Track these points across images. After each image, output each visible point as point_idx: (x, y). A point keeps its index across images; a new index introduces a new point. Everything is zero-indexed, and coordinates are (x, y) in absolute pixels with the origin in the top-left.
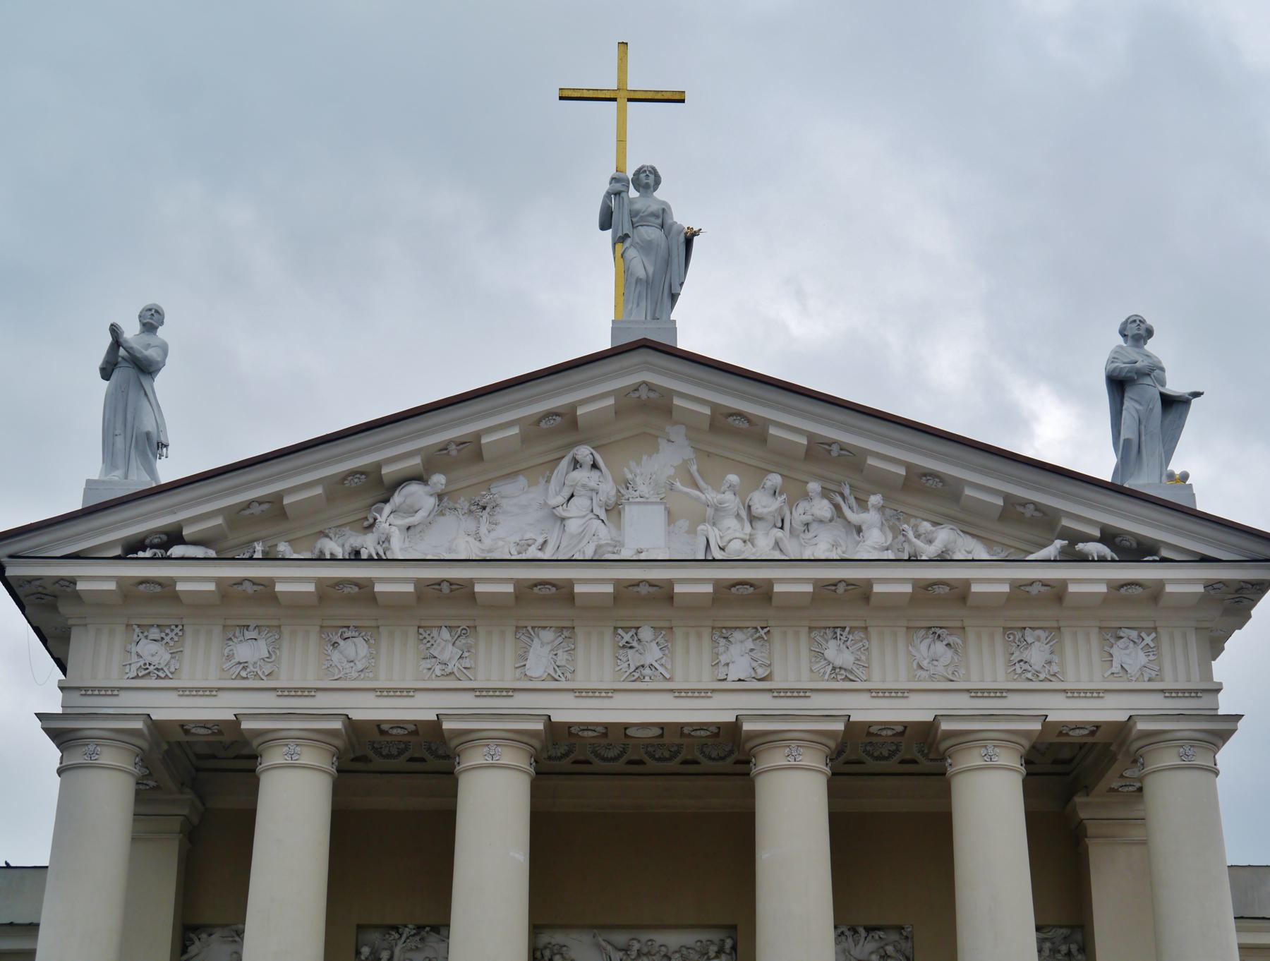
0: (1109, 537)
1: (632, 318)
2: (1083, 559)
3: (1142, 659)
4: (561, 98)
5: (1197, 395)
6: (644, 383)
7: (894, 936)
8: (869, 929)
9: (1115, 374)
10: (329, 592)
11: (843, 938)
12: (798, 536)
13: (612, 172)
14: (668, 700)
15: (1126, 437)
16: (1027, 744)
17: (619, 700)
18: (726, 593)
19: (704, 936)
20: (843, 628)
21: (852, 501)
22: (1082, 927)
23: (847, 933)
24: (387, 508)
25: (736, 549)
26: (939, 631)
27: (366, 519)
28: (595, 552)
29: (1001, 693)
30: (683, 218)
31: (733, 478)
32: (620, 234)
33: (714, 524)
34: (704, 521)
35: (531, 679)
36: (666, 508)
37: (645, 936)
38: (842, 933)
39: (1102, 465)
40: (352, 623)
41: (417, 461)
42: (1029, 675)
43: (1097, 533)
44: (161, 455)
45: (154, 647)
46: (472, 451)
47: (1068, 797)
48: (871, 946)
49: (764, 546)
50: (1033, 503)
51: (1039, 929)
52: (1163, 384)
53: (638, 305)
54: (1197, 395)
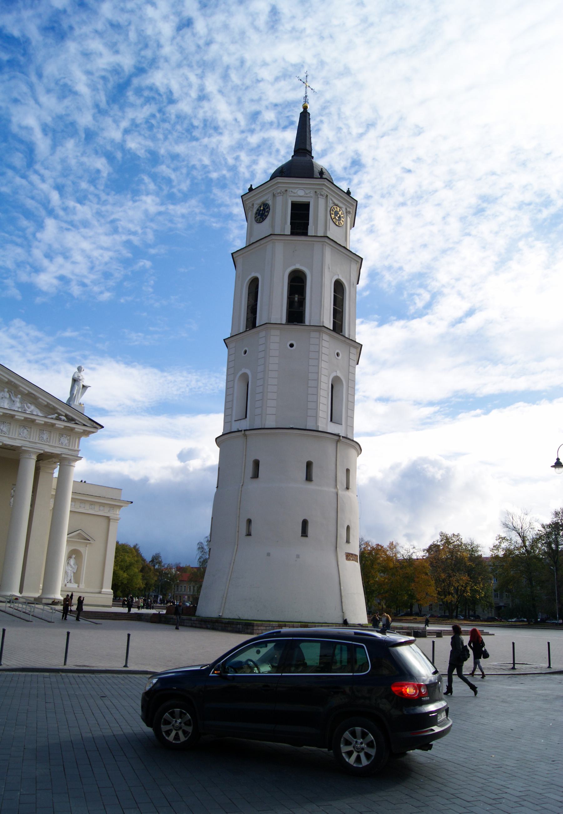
0: (66, 416)
3: (66, 441)
5: (90, 387)
20: (6, 422)
21: (13, 394)
29: (35, 443)
42: (43, 440)
43: (64, 415)
52: (83, 382)
54: (90, 387)
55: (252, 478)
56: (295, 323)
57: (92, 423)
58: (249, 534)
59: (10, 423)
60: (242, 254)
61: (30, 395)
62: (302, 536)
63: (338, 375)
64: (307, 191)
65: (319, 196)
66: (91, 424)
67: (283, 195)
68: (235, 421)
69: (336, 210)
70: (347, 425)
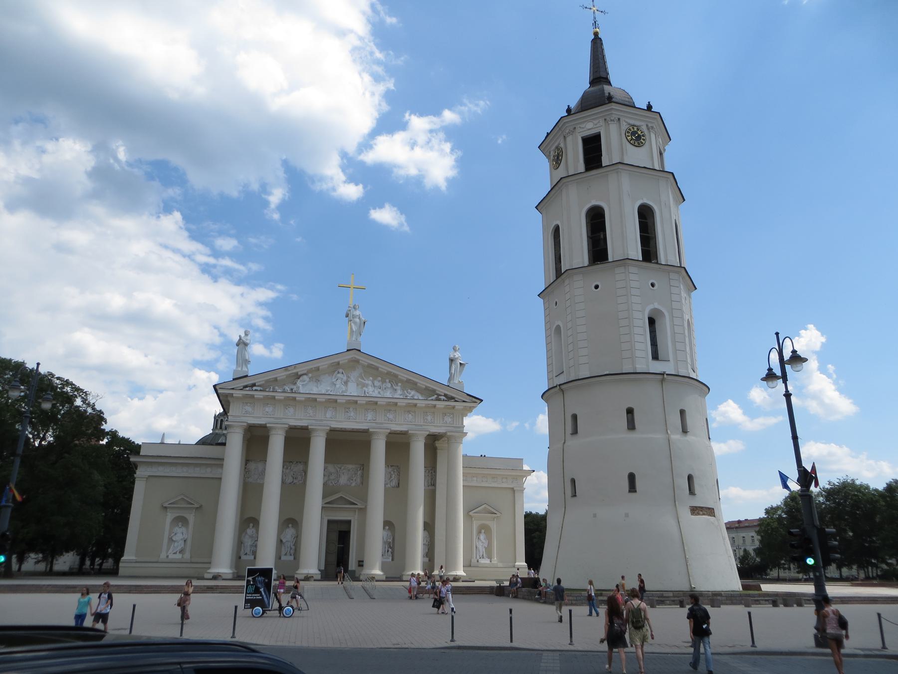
0: (445, 395)
2: (440, 400)
3: (450, 420)
8: (391, 466)
10: (287, 398)
18: (368, 403)
29: (421, 425)
31: (371, 378)
33: (367, 387)
34: (364, 386)
35: (326, 417)
46: (318, 369)
47: (435, 441)
49: (376, 394)
55: (572, 434)
56: (596, 263)
57: (471, 398)
58: (574, 495)
59: (395, 411)
60: (544, 205)
61: (408, 381)
62: (630, 491)
63: (656, 307)
64: (595, 122)
65: (609, 123)
66: (470, 400)
67: (572, 134)
68: (556, 376)
69: (632, 130)
70: (676, 361)
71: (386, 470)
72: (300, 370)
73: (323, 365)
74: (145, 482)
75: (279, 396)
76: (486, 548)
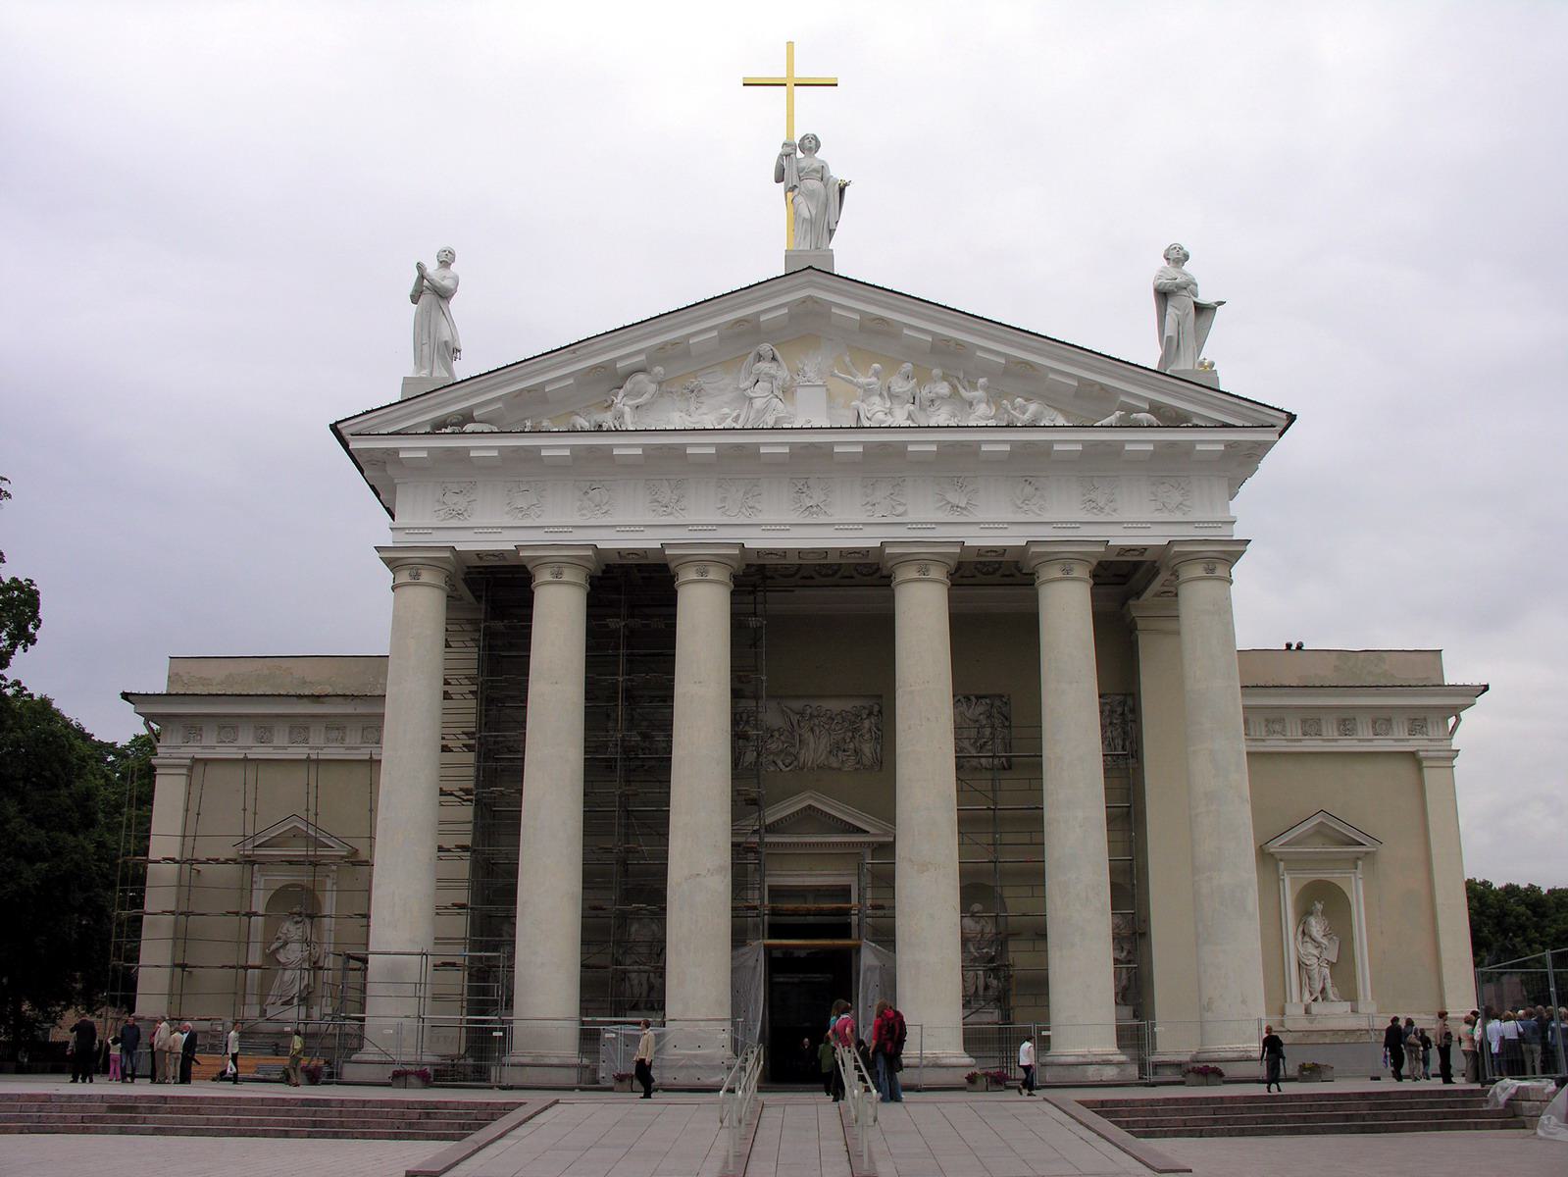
0: (1155, 409)
1: (801, 248)
4: (744, 85)
5: (1221, 303)
6: (809, 296)
7: (998, 703)
8: (978, 697)
9: (1161, 288)
11: (960, 704)
12: (925, 410)
13: (784, 139)
14: (829, 532)
15: (1169, 334)
16: (1095, 563)
17: (795, 532)
19: (858, 703)
21: (966, 384)
22: (1133, 695)
23: (962, 700)
24: (621, 393)
25: (880, 418)
26: (1030, 479)
27: (607, 401)
28: (776, 422)
30: (837, 173)
31: (876, 366)
32: (790, 185)
36: (827, 390)
37: (815, 704)
38: (959, 700)
39: (1150, 356)
40: (595, 478)
41: (643, 357)
43: (1148, 408)
44: (456, 358)
45: (456, 499)
47: (1124, 603)
48: (981, 709)
49: (900, 419)
50: (1101, 384)
51: (1100, 696)
52: (1196, 296)
53: (805, 238)
54: (1221, 303)
71: (962, 714)
72: (622, 356)
73: (702, 333)
74: (183, 780)
75: (556, 447)
76: (1332, 965)
